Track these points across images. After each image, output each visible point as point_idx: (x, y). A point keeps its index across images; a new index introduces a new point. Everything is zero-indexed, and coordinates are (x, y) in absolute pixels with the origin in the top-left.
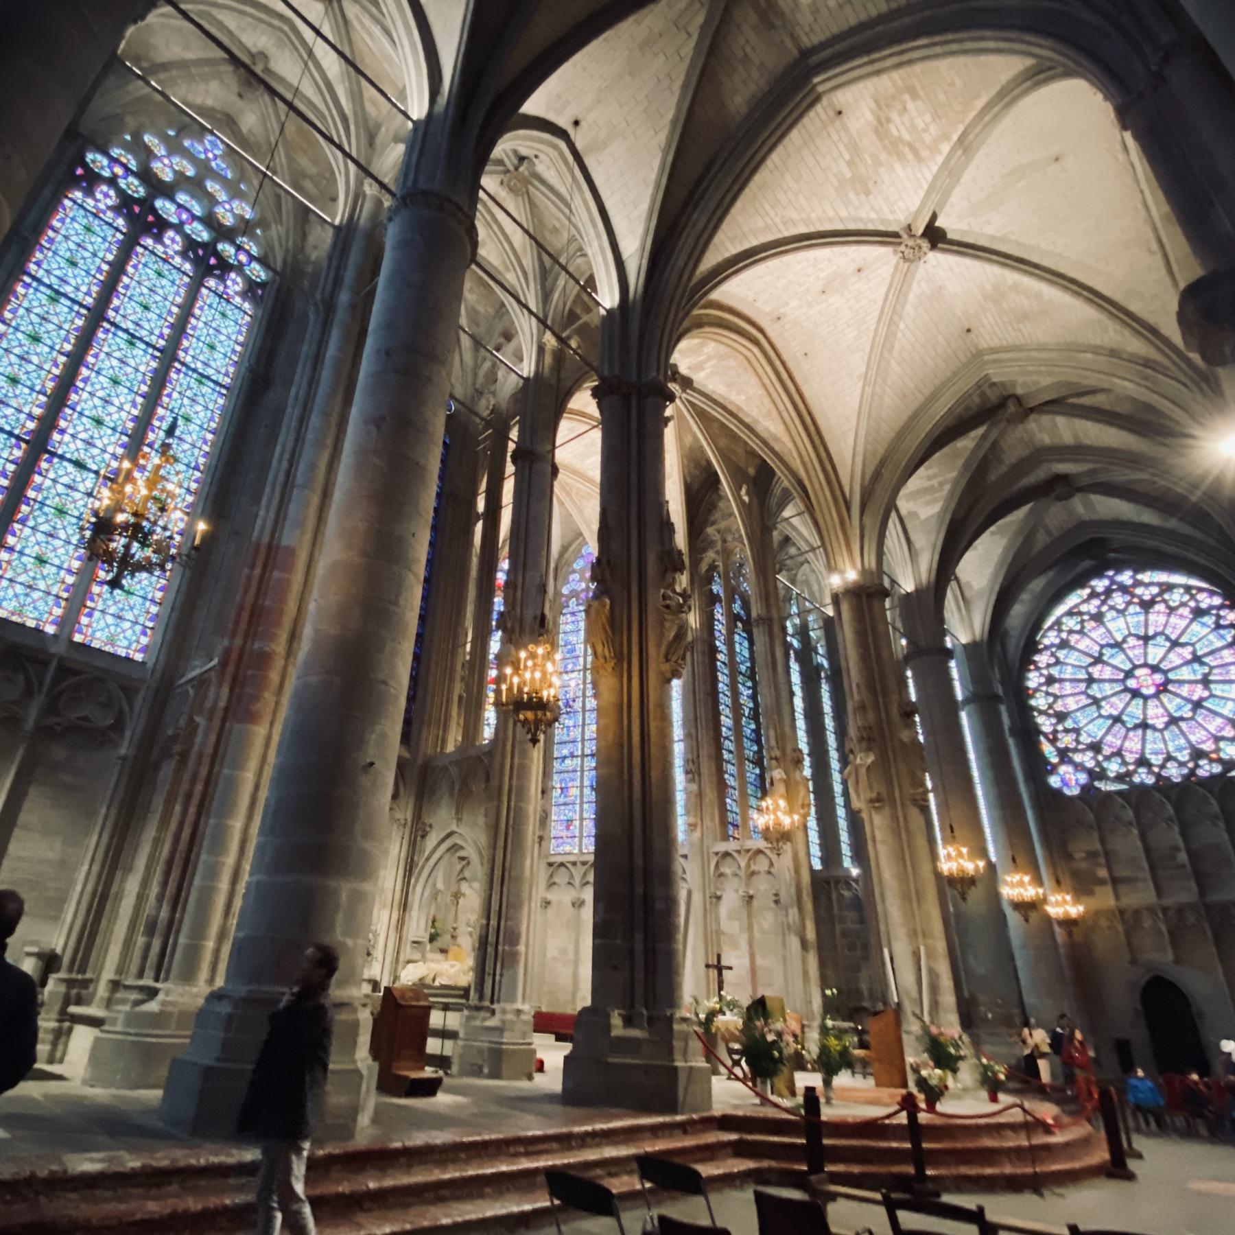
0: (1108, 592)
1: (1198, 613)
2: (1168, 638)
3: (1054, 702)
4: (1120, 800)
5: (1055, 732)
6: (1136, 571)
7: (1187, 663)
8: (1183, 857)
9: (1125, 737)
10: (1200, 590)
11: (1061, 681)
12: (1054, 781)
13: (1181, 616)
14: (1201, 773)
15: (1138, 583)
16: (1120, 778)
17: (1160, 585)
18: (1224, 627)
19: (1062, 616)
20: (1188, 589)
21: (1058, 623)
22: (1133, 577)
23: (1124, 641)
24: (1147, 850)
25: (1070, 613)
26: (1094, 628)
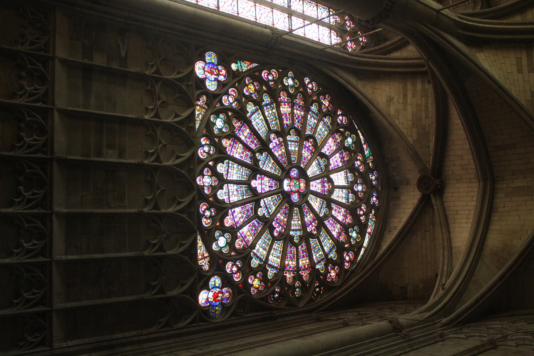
0: (366, 182)
1: (339, 247)
2: (326, 217)
3: (289, 95)
4: (185, 114)
5: (262, 82)
6: (377, 209)
7: (304, 226)
8: (111, 157)
9: (246, 147)
10: (357, 254)
11: (307, 109)
12: (211, 57)
13: (339, 234)
14: (203, 207)
15: (370, 207)
16: (209, 125)
17: (366, 226)
18: (326, 265)
19: (357, 135)
20: (359, 245)
21: (353, 132)
22: (373, 206)
23: (331, 181)
24: (123, 121)
25: (357, 142)
26: (342, 158)
